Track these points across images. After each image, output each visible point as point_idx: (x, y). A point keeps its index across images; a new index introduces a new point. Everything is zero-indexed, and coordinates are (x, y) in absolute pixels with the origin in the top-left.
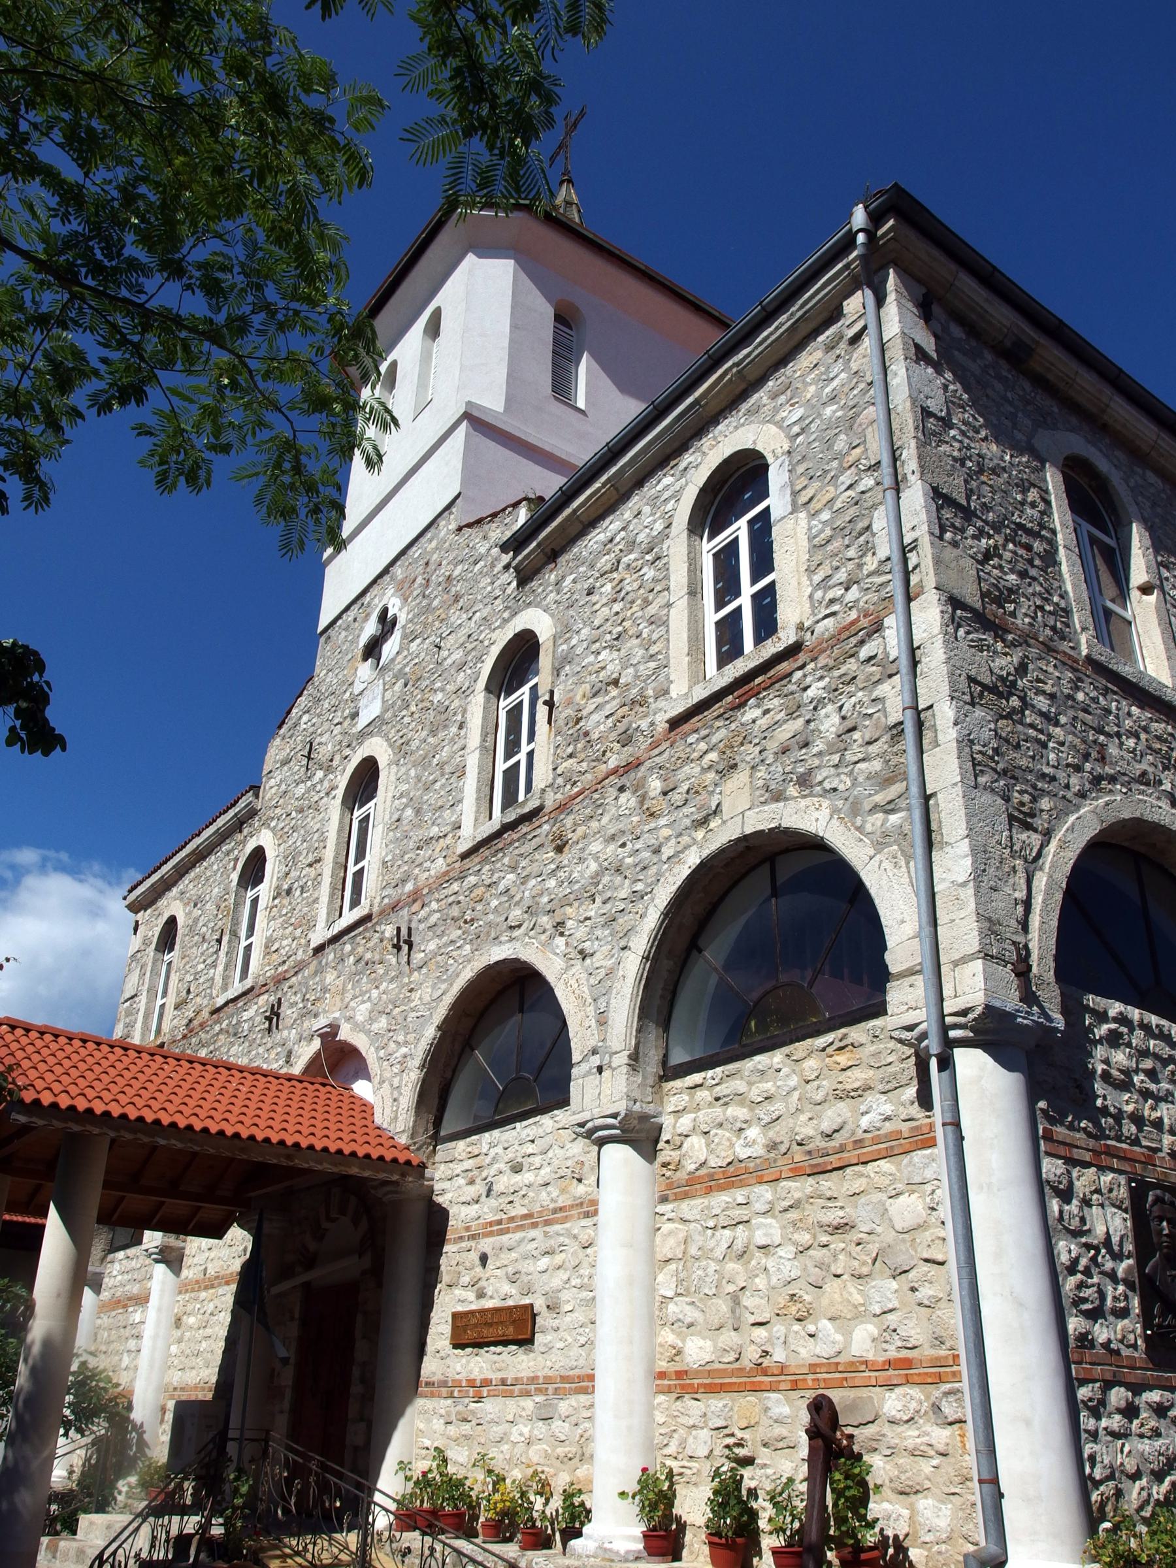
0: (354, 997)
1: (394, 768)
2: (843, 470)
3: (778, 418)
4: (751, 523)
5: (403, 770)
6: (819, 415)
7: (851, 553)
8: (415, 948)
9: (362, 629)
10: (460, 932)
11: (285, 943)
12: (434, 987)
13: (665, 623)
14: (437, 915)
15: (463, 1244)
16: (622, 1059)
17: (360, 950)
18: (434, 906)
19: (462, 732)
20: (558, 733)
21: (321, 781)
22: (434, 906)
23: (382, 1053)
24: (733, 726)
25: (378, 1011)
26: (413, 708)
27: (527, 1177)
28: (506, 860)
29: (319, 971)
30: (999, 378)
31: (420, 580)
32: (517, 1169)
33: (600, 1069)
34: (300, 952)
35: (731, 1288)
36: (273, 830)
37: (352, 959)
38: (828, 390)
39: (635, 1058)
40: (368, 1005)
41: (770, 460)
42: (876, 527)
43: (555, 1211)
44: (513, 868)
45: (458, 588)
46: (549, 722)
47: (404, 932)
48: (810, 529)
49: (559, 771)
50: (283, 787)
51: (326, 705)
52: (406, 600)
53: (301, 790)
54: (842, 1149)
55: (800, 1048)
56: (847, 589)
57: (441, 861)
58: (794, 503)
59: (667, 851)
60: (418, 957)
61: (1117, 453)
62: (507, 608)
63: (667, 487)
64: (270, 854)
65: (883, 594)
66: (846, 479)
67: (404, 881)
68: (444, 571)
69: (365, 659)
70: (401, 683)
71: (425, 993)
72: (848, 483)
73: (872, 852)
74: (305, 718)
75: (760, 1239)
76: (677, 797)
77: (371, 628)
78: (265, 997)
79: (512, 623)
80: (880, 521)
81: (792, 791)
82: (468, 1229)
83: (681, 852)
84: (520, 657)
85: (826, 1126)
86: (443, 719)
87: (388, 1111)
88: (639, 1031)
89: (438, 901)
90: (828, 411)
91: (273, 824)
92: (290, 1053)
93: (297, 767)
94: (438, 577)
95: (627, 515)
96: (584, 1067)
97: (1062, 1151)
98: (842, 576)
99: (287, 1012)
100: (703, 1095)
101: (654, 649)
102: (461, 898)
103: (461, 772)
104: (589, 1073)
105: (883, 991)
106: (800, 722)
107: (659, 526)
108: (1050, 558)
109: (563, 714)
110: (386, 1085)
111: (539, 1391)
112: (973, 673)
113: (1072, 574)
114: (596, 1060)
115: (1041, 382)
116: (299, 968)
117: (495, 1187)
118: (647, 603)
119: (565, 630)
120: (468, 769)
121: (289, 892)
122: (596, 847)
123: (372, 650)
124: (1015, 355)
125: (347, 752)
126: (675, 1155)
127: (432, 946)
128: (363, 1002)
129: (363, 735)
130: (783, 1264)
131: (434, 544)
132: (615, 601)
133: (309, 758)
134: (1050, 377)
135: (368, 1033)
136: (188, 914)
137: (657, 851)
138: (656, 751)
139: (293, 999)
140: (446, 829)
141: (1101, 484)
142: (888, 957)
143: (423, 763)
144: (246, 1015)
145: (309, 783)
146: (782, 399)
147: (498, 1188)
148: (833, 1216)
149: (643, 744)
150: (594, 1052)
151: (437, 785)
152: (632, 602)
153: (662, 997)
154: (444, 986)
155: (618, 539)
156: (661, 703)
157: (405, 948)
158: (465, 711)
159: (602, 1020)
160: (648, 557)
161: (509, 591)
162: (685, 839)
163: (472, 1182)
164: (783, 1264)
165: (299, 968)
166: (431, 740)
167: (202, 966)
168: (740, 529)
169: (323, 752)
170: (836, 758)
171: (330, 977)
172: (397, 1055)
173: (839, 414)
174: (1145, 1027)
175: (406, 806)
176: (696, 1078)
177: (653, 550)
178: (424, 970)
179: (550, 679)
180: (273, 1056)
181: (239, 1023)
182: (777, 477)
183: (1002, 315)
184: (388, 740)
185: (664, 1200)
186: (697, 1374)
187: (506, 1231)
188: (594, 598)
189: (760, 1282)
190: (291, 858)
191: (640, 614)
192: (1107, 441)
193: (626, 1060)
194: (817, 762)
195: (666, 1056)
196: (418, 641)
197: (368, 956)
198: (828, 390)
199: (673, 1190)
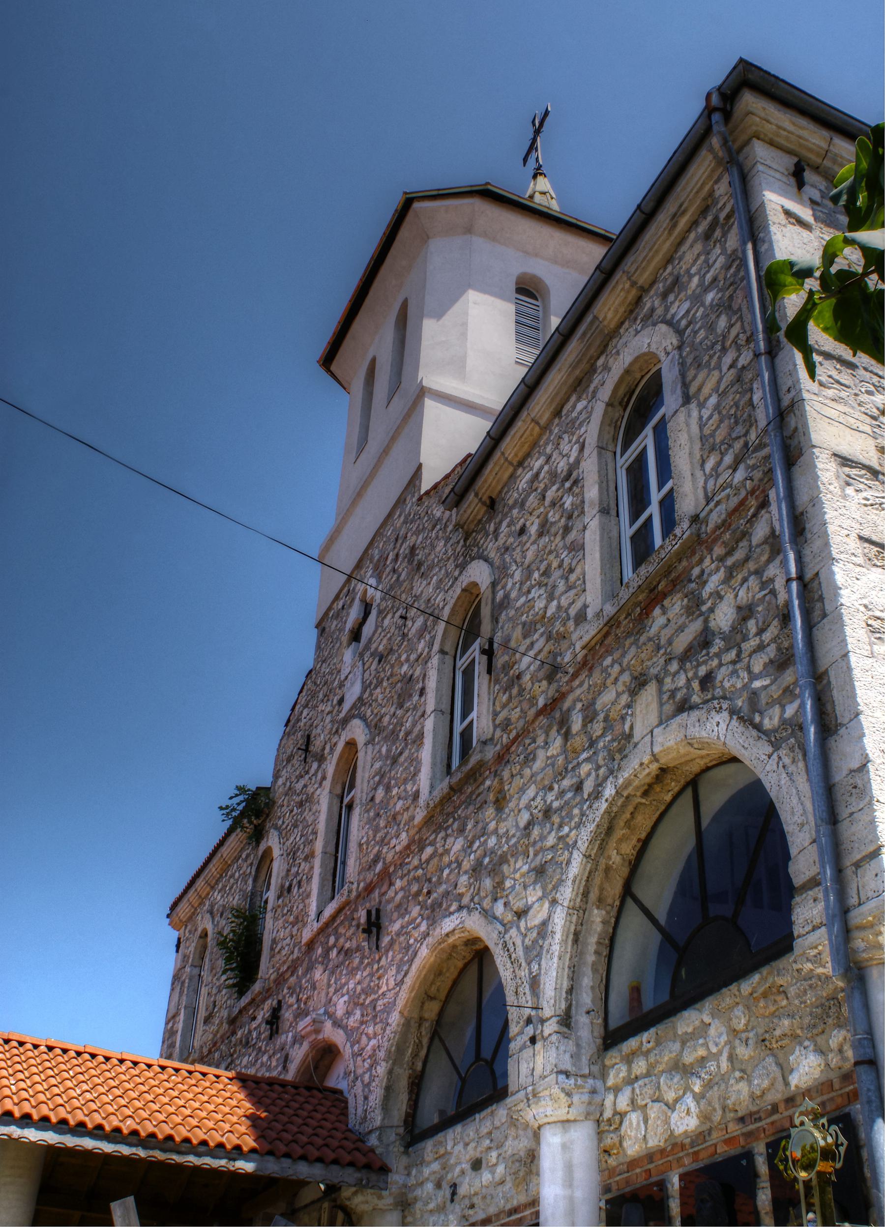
0: (336, 991)
2: (724, 350)
3: (669, 316)
4: (655, 428)
5: (377, 747)
8: (384, 932)
9: (348, 614)
11: (285, 942)
13: (582, 548)
14: (401, 894)
17: (342, 940)
20: (497, 681)
25: (355, 1002)
26: (385, 684)
27: (486, 1177)
28: (455, 826)
29: (310, 969)
31: (391, 557)
33: (533, 1040)
37: (335, 951)
39: (566, 1020)
40: (346, 998)
45: (420, 555)
46: (489, 672)
48: (701, 418)
49: (497, 722)
50: (288, 784)
55: (727, 997)
59: (588, 786)
60: (385, 940)
64: (276, 853)
67: (375, 861)
69: (349, 644)
71: (390, 979)
73: (770, 749)
77: (354, 613)
86: (408, 689)
87: (360, 1111)
89: (402, 878)
92: (286, 1058)
94: (404, 549)
99: (287, 1015)
104: (523, 1047)
105: (789, 910)
110: (359, 1083)
112: (866, 533)
114: (530, 1031)
116: (293, 969)
123: (356, 635)
127: (396, 926)
128: (343, 996)
129: (345, 721)
131: (402, 518)
135: (344, 1028)
136: (215, 926)
142: (792, 869)
144: (254, 1025)
147: (462, 1190)
153: (597, 953)
157: (374, 930)
159: (535, 983)
160: (567, 485)
161: (458, 549)
165: (293, 969)
168: (647, 439)
169: (317, 745)
170: (733, 654)
171: (318, 974)
172: (369, 1048)
173: (720, 295)
177: (571, 479)
180: (274, 1063)
181: (250, 1032)
188: (524, 538)
190: (292, 854)
196: (390, 616)
197: (347, 945)
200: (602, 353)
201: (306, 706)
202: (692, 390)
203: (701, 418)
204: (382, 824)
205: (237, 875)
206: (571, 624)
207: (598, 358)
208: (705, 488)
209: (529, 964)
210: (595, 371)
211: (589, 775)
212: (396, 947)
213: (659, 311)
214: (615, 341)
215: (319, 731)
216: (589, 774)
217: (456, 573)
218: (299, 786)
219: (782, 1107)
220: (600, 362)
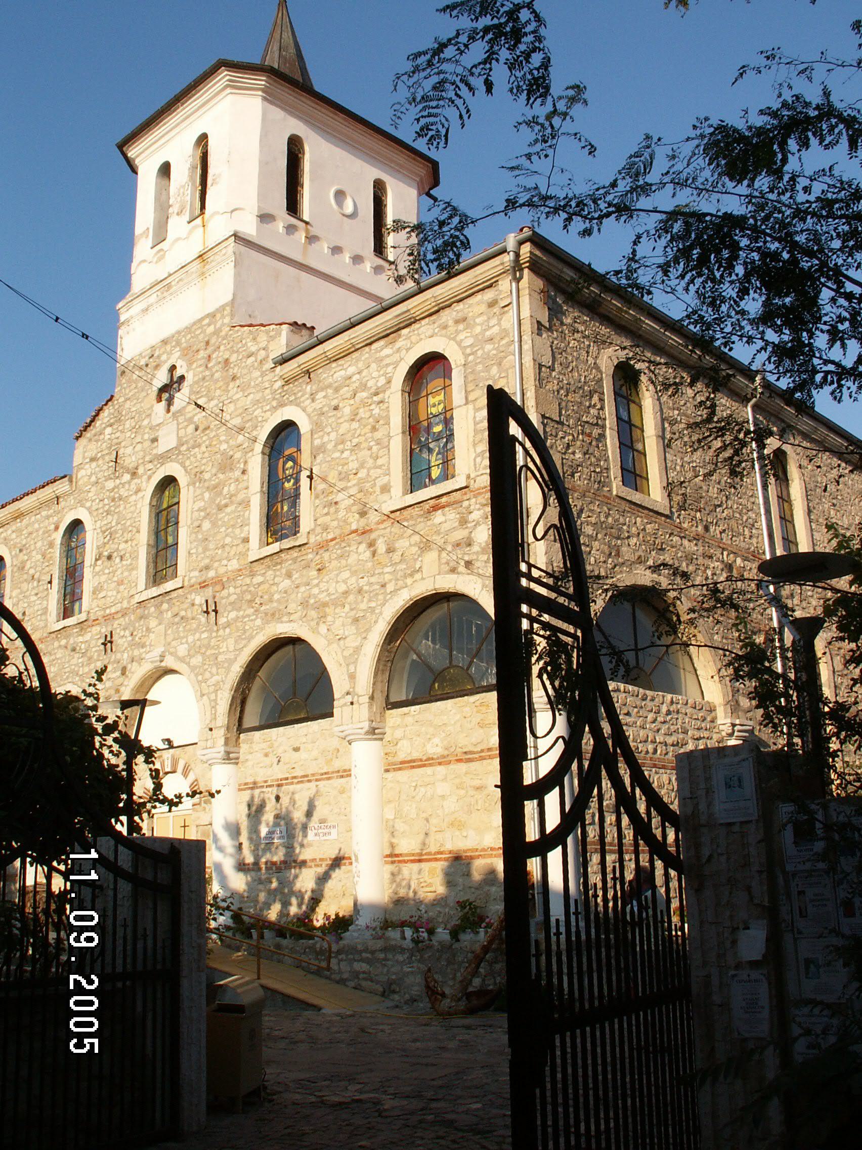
1: (191, 488)
3: (458, 339)
5: (198, 492)
6: (482, 348)
10: (252, 610)
12: (236, 642)
14: (235, 596)
15: (264, 790)
16: (365, 699)
18: (232, 590)
19: (245, 477)
20: (317, 497)
21: (129, 482)
22: (232, 590)
23: (200, 678)
24: (429, 523)
25: (194, 650)
26: (203, 448)
32: (297, 749)
33: (352, 703)
34: (125, 602)
35: (424, 815)
36: (89, 509)
38: (488, 333)
39: (372, 698)
43: (322, 774)
44: (289, 575)
46: (311, 489)
47: (211, 603)
48: (475, 417)
49: (319, 522)
51: (127, 426)
52: (191, 364)
53: (110, 484)
54: (482, 751)
57: (235, 562)
58: (466, 398)
59: (390, 587)
60: (222, 620)
62: (274, 399)
63: (388, 356)
64: (88, 524)
67: (207, 568)
68: (223, 354)
70: (192, 427)
74: (108, 430)
75: (440, 792)
76: (396, 557)
78: (98, 628)
79: (279, 412)
81: (462, 569)
82: (266, 782)
83: (399, 590)
84: (284, 434)
85: (474, 740)
88: (374, 684)
89: (235, 588)
90: (488, 347)
91: (88, 504)
93: (105, 466)
95: (360, 365)
96: (342, 702)
100: (409, 720)
101: (380, 462)
102: (252, 589)
103: (246, 504)
104: (345, 705)
106: (467, 531)
107: (382, 381)
108: (602, 436)
109: (320, 486)
111: (317, 866)
113: (612, 444)
114: (349, 698)
117: (282, 759)
118: (374, 429)
119: (317, 427)
120: (252, 503)
121: (109, 558)
122: (346, 575)
125: (150, 466)
126: (393, 749)
127: (233, 615)
129: (164, 458)
130: (451, 805)
132: (353, 420)
133: (116, 462)
134: (611, 316)
135: (188, 664)
137: (383, 586)
138: (382, 526)
139: (122, 633)
140: (235, 542)
143: (216, 489)
145: (118, 481)
146: (461, 327)
148: (477, 783)
149: (373, 517)
150: (348, 693)
151: (229, 510)
152: (365, 426)
154: (244, 642)
155: (354, 379)
156: (385, 497)
158: (246, 462)
159: (352, 677)
160: (375, 399)
162: (400, 583)
163: (266, 755)
164: (451, 805)
166: (221, 476)
167: (34, 598)
171: (153, 623)
173: (494, 352)
175: (205, 518)
176: (405, 710)
178: (228, 630)
179: (309, 460)
184: (184, 467)
185: (387, 771)
186: (407, 855)
187: (292, 783)
188: (339, 414)
189: (440, 812)
190: (109, 534)
191: (370, 435)
193: (367, 700)
194: (475, 557)
195: (387, 696)
197: (183, 613)
198: (488, 333)
199: (393, 766)
201: (111, 426)
202: (471, 398)
203: (475, 417)
204: (212, 546)
205: (36, 526)
206: (378, 489)
207: (404, 328)
208: (475, 460)
209: (348, 665)
210: (400, 336)
211: (390, 581)
212: (233, 627)
213: (452, 329)
215: (129, 450)
216: (390, 581)
217: (274, 403)
218: (110, 484)
220: (405, 332)
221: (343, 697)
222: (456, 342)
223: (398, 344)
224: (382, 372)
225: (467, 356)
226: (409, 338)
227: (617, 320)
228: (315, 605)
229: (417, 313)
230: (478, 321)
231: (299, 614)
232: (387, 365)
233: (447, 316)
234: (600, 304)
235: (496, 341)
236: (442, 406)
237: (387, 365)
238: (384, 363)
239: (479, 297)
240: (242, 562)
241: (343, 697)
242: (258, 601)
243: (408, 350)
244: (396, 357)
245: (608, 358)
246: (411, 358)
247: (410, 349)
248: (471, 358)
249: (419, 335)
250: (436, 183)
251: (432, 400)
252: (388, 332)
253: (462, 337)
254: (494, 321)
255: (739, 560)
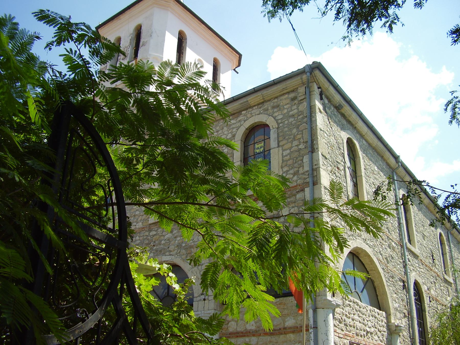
3: (274, 115)
7: (296, 165)
14: (139, 241)
22: (137, 238)
30: (334, 115)
33: (204, 300)
38: (291, 113)
41: (271, 128)
42: (304, 161)
48: (282, 154)
56: (294, 176)
61: (357, 135)
63: (234, 124)
65: (305, 181)
66: (295, 143)
72: (296, 144)
80: (306, 159)
89: (139, 237)
90: (291, 120)
96: (198, 298)
97: (337, 335)
98: (292, 171)
102: (149, 238)
104: (200, 300)
114: (203, 297)
115: (343, 115)
124: (338, 108)
134: (345, 114)
140: (142, 214)
141: (354, 145)
146: (275, 110)
174: (354, 302)
182: (273, 135)
183: (338, 98)
192: (355, 131)
198: (291, 113)
200: (245, 110)
202: (281, 144)
203: (282, 154)
213: (270, 111)
214: (250, 110)
219: (282, 329)
220: (243, 112)
221: (199, 296)
222: (273, 117)
223: (239, 119)
224: (230, 132)
225: (278, 124)
226: (245, 115)
227: (348, 116)
228: (185, 247)
229: (252, 103)
230: (285, 107)
231: (176, 251)
232: (233, 128)
233: (267, 105)
234: (342, 107)
235: (296, 116)
236: (262, 149)
237: (233, 128)
238: (232, 127)
239: (287, 96)
240: (145, 224)
241: (199, 296)
242: (152, 244)
243: (245, 121)
244: (238, 124)
245: (345, 135)
246: (248, 124)
247: (246, 120)
248: (281, 125)
249: (251, 114)
250: (239, 65)
251: (257, 146)
252: (235, 112)
253: (277, 115)
254: (295, 107)
255: (393, 243)
